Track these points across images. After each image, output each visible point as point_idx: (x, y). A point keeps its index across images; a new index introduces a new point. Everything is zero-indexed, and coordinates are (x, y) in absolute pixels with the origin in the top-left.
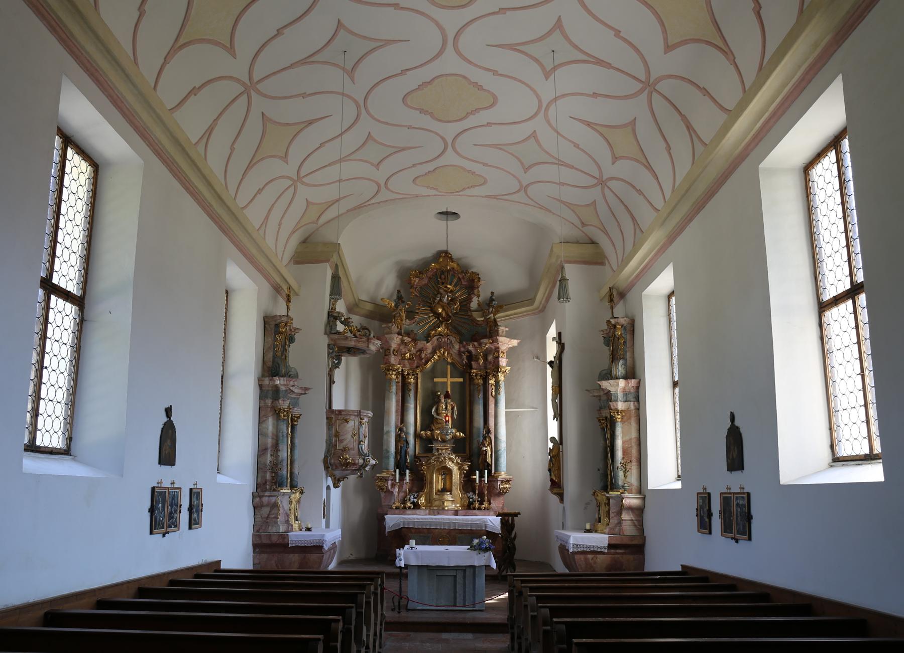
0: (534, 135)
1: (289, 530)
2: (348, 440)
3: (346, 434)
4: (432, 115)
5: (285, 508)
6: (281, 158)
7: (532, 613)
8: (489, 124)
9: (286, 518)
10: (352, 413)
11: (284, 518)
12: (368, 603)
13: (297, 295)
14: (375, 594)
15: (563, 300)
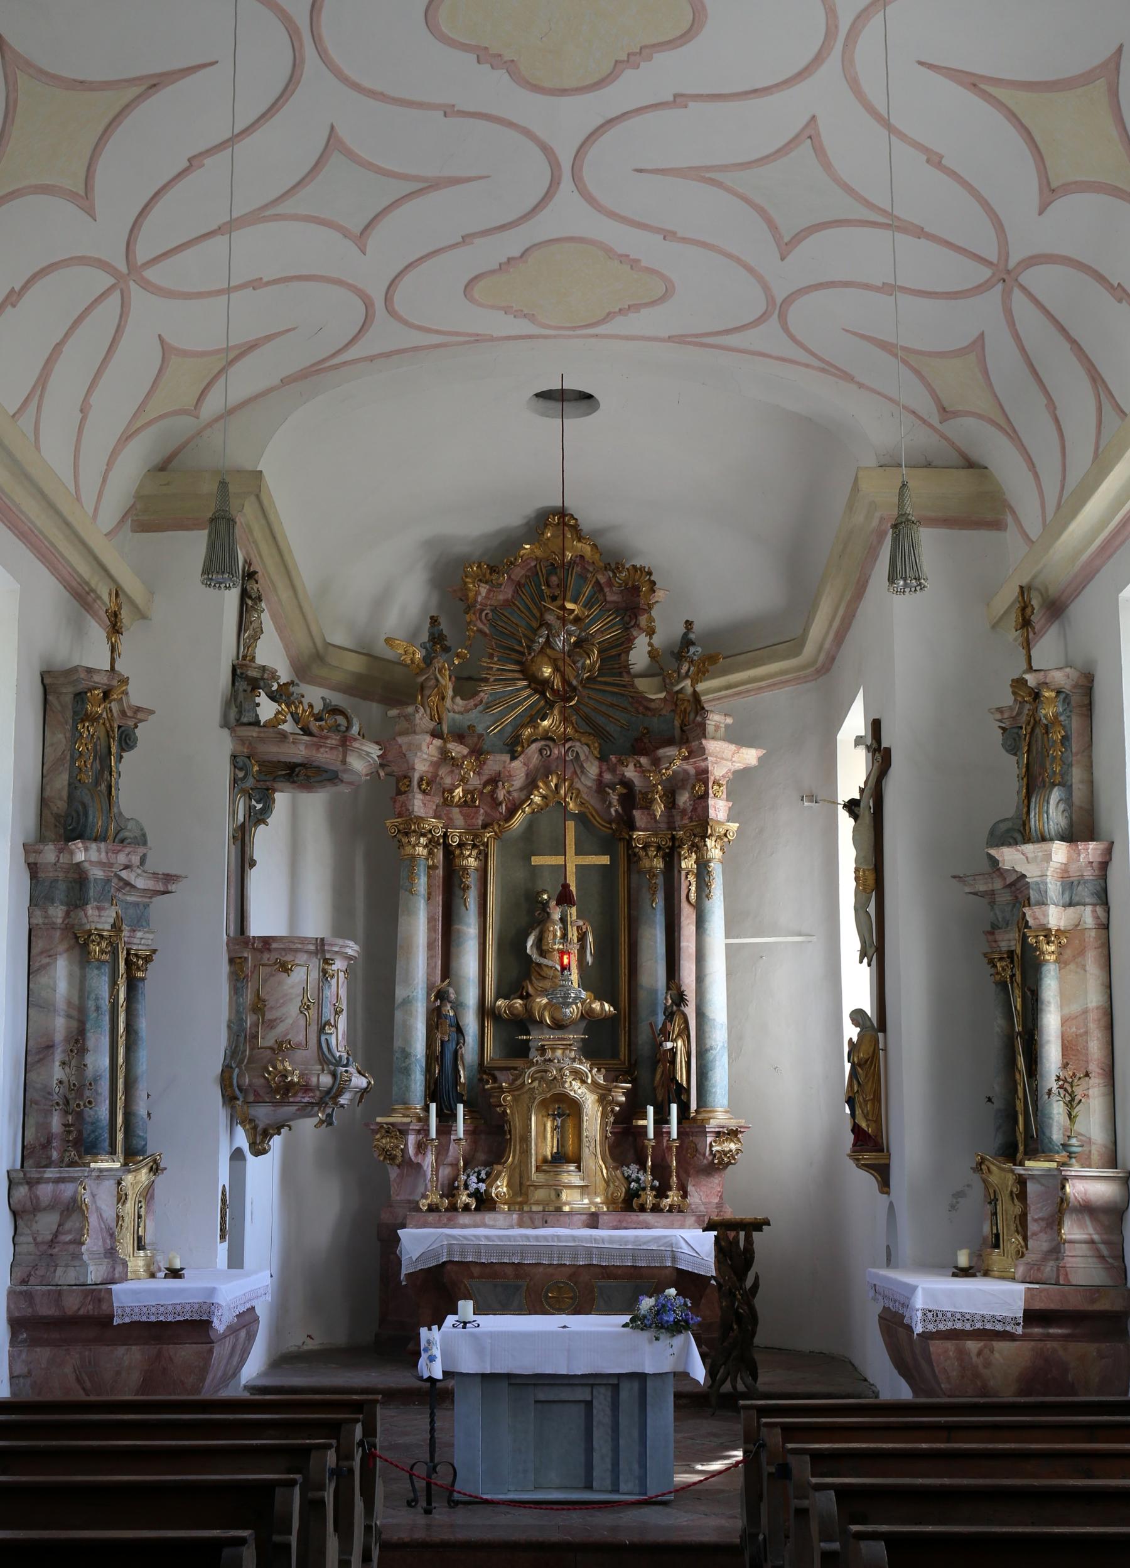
0: (810, 133)
1: (117, 1275)
2: (290, 1021)
3: (283, 1004)
4: (511, 68)
5: (105, 1215)
6: (71, 196)
7: (822, 1544)
8: (680, 100)
9: (108, 1242)
10: (299, 946)
11: (100, 1243)
12: (312, 1507)
13: (144, 617)
14: (342, 1475)
15: (906, 585)
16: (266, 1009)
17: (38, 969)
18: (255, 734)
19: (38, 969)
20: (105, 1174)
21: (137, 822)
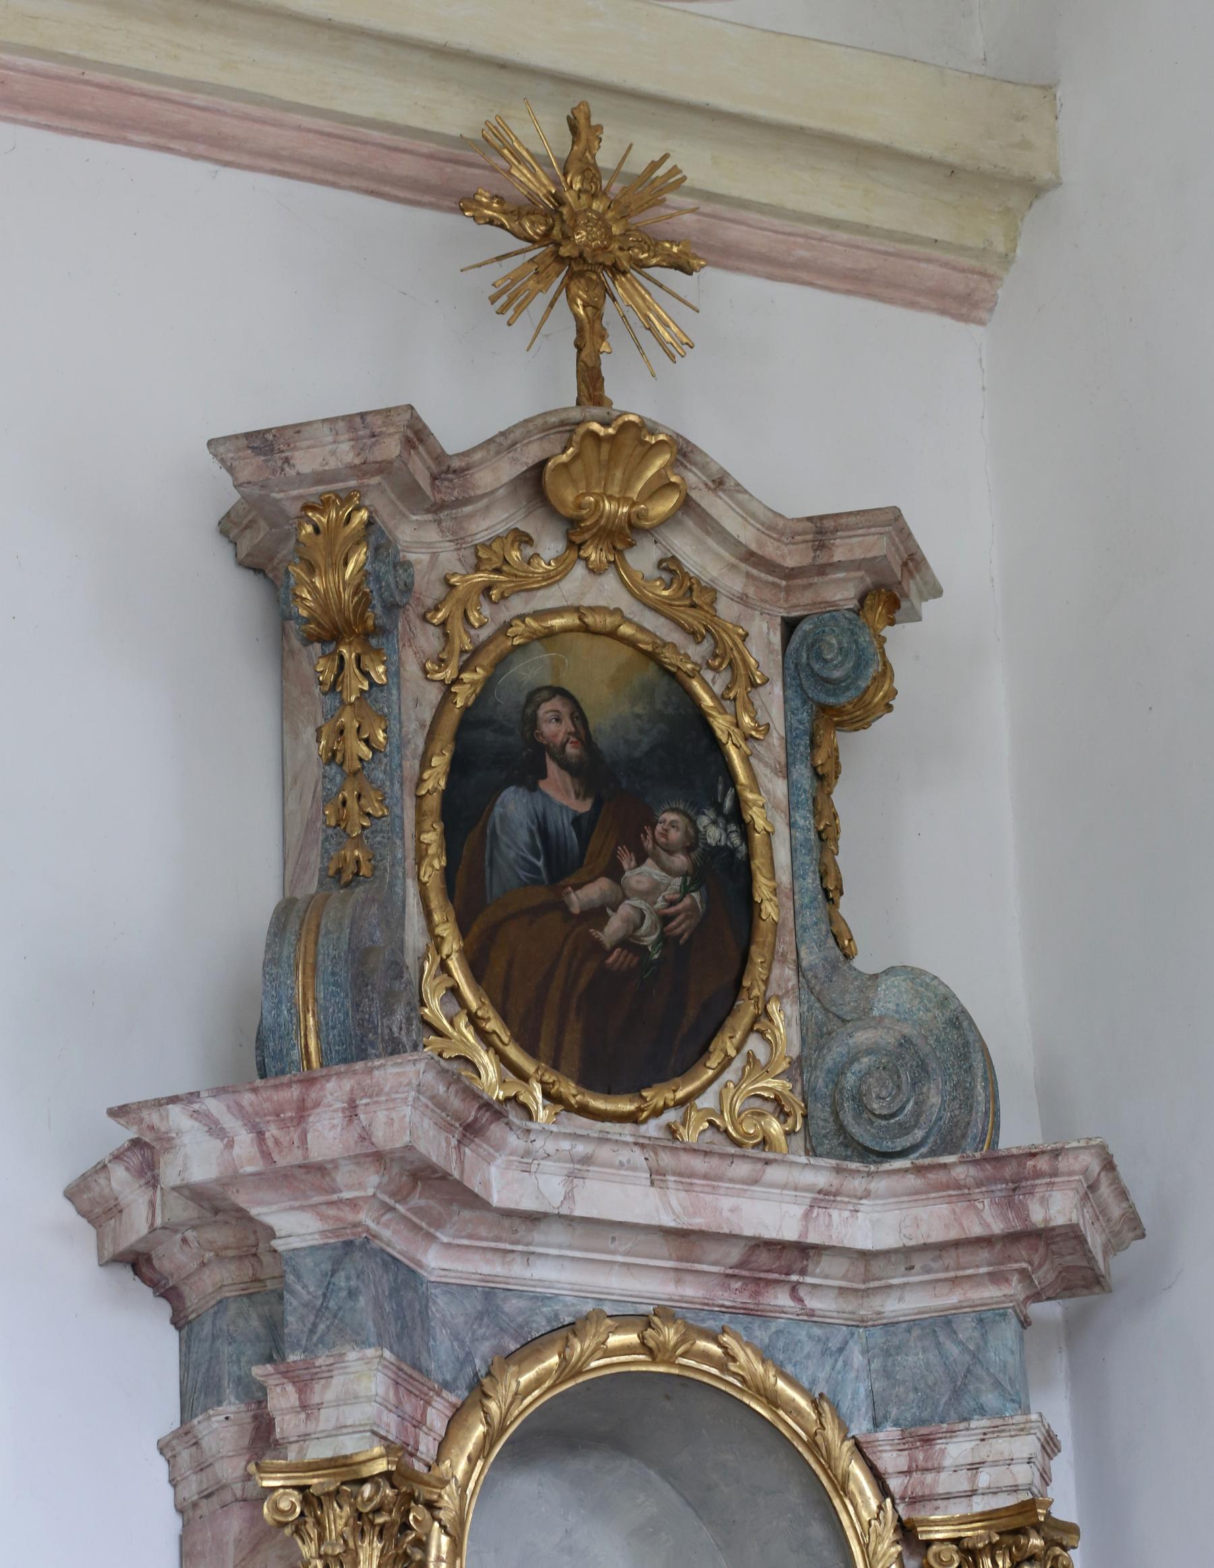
13: (1034, 189)
21: (914, 975)
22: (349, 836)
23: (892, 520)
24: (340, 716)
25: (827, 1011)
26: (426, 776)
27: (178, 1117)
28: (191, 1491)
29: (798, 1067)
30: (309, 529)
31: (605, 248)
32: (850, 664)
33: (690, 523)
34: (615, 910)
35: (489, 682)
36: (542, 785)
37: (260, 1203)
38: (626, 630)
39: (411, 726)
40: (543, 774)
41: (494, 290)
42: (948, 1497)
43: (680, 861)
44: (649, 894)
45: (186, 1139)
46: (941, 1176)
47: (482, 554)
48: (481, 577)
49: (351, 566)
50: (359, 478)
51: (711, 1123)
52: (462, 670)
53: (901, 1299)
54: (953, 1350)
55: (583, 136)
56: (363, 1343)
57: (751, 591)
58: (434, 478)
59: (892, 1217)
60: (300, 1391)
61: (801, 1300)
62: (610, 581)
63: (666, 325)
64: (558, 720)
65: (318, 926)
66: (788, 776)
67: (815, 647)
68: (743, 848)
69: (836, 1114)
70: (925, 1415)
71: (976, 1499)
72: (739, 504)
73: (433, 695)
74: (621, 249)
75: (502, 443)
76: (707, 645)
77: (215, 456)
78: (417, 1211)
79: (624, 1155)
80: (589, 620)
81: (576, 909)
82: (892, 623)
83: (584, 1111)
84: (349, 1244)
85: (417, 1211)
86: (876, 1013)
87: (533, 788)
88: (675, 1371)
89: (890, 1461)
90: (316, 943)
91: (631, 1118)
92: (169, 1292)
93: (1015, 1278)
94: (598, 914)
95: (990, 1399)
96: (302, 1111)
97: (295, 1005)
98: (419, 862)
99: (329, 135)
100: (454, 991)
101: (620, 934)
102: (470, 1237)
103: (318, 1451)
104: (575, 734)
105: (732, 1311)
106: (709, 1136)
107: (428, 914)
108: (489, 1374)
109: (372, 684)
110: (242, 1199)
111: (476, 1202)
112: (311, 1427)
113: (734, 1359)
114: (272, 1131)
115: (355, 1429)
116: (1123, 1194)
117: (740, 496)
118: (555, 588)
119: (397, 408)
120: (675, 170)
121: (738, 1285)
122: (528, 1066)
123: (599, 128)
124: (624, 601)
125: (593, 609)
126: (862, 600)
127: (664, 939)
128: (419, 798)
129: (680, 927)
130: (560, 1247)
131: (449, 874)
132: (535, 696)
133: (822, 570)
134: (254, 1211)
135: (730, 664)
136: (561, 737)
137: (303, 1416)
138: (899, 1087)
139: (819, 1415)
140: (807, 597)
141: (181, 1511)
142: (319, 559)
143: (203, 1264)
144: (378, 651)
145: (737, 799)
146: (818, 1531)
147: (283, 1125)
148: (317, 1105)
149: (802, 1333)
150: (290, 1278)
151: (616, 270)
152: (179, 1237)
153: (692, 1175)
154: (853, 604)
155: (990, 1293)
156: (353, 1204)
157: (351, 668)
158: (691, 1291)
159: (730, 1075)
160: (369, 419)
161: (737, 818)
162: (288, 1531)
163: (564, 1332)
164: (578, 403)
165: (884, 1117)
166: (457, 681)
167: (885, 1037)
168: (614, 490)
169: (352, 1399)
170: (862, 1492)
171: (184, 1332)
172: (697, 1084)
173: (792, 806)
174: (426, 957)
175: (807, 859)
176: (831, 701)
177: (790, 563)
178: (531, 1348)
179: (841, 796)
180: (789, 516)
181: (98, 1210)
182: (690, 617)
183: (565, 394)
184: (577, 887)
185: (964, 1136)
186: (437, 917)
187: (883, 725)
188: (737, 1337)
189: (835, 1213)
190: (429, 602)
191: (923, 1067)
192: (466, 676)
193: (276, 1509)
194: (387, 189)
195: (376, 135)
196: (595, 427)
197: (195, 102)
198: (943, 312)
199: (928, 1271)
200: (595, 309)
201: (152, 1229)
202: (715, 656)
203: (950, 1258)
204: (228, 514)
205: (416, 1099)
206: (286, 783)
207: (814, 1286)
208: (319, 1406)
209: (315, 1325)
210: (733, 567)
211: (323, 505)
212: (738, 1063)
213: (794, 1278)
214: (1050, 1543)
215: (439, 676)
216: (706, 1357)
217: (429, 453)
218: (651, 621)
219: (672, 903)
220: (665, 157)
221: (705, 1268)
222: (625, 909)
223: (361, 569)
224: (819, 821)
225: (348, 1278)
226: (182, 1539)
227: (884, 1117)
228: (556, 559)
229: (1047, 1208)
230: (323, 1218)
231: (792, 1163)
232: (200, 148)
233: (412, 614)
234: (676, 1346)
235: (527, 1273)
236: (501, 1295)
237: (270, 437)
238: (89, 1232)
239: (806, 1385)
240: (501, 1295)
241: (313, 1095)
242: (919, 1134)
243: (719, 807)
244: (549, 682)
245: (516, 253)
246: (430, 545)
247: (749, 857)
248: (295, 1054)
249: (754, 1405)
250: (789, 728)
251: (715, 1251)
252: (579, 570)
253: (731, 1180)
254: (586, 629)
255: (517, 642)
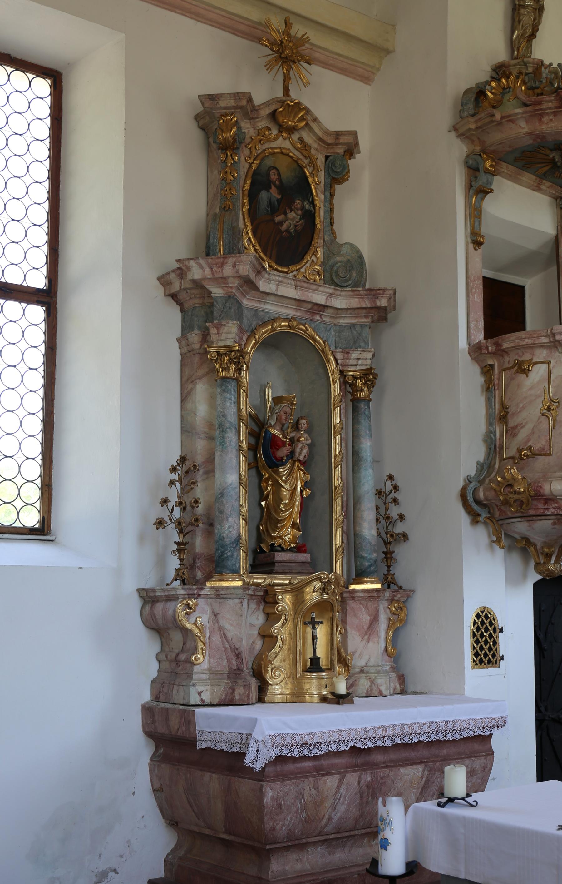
2: (530, 426)
3: (523, 407)
5: (229, 635)
10: (530, 341)
13: (388, 52)
16: (509, 416)
17: (186, 396)
18: (473, 126)
19: (186, 396)
20: (222, 592)
21: (351, 245)
22: (227, 199)
23: (354, 134)
24: (226, 169)
25: (330, 251)
26: (245, 186)
27: (192, 263)
28: (185, 350)
29: (322, 264)
30: (222, 121)
31: (291, 56)
32: (341, 168)
33: (307, 129)
34: (285, 223)
35: (260, 164)
36: (270, 190)
37: (209, 285)
38: (291, 154)
39: (242, 173)
40: (271, 188)
41: (265, 64)
42: (351, 365)
43: (300, 212)
44: (293, 219)
45: (194, 269)
46: (357, 293)
47: (260, 131)
48: (259, 137)
49: (232, 132)
50: (234, 109)
51: (304, 275)
52: (254, 160)
53: (344, 320)
54: (355, 333)
55: (288, 25)
56: (232, 320)
57: (319, 148)
58: (251, 111)
59: (345, 301)
60: (217, 330)
61: (322, 318)
62: (287, 142)
63: (304, 78)
64: (275, 175)
65: (224, 220)
66: (324, 194)
67: (333, 163)
68: (313, 211)
69: (331, 276)
70: (347, 347)
71: (357, 366)
72: (319, 125)
73: (247, 166)
74: (296, 57)
75: (267, 104)
76: (308, 160)
77: (199, 99)
78: (244, 290)
79: (290, 281)
80: (283, 151)
81: (276, 222)
82: (350, 159)
83: (276, 270)
84: (229, 297)
85: (244, 290)
86: (341, 253)
87: (268, 191)
88: (295, 332)
89: (339, 356)
90: (223, 224)
91: (287, 273)
92: (180, 304)
93: (370, 317)
94: (281, 223)
95: (362, 344)
96: (222, 265)
97: (218, 239)
98: (243, 206)
99: (225, 17)
100: (249, 239)
101: (286, 229)
102: (253, 297)
103: (221, 344)
104: (278, 179)
105: (307, 319)
106: (303, 278)
107: (244, 220)
108: (255, 329)
109: (234, 162)
110: (205, 284)
111: (256, 289)
112: (219, 338)
113: (308, 330)
114: (215, 269)
115: (230, 339)
116: (395, 301)
117: (320, 124)
118: (275, 142)
119: (247, 92)
120: (308, 37)
121: (309, 313)
122: (265, 258)
123: (292, 24)
124: (290, 147)
125: (284, 148)
126: (345, 152)
127: (295, 231)
128: (243, 191)
129: (299, 228)
130: (272, 301)
131: (249, 210)
132: (270, 168)
133: (336, 144)
134: (207, 287)
135: (313, 166)
136: (275, 179)
137: (218, 335)
138: (346, 271)
139: (325, 345)
140: (331, 151)
141: (181, 354)
142: (224, 128)
143: (191, 298)
144: (236, 154)
145: (313, 198)
146: (321, 371)
147: (218, 267)
148: (226, 263)
149: (321, 326)
150: (215, 303)
151: (294, 62)
152: (186, 291)
153: (303, 287)
154: (342, 154)
155: (364, 320)
156: (231, 287)
157: (229, 157)
158: (299, 314)
159: (308, 264)
160: (239, 94)
161: (313, 203)
162: (214, 361)
163: (272, 321)
164: (284, 96)
165: (343, 278)
166: (253, 163)
167: (343, 259)
168: (291, 119)
169: (229, 332)
170: (332, 363)
171: (183, 313)
172: (301, 266)
173: (325, 202)
174: (244, 230)
175: (328, 215)
176: (336, 177)
177: (329, 142)
178: (264, 324)
179: (335, 201)
180: (330, 130)
181: (165, 283)
182: (305, 153)
183: (280, 93)
184: (277, 216)
185: (360, 284)
186: (246, 220)
187: (345, 184)
188: (308, 325)
189: (333, 299)
190: (247, 143)
191: (352, 267)
192: (255, 162)
193: (211, 355)
194: (236, 33)
195: (236, 18)
196: (289, 102)
197: (193, 3)
198: (361, 81)
199: (351, 314)
200: (288, 71)
201: (181, 288)
202: (310, 163)
203: (356, 311)
204: (198, 114)
205: (250, 264)
206: (209, 183)
207: (326, 315)
208: (222, 333)
209: (221, 315)
210: (315, 141)
211: (226, 115)
212: (310, 262)
213: (321, 313)
214: (374, 378)
215: (248, 161)
216: (301, 329)
217: (251, 104)
218: (296, 153)
219: (297, 222)
220: (306, 33)
221: (303, 309)
222: (287, 223)
223: (234, 133)
224: (331, 206)
225: (229, 304)
226: (181, 361)
227: (343, 278)
228: (276, 135)
229: (381, 302)
230: (224, 290)
231: (325, 287)
232: (193, 16)
233: (243, 145)
234: (296, 326)
235: (264, 307)
236: (258, 311)
237: (214, 96)
238: (162, 288)
239: (322, 337)
240: (258, 311)
241: (226, 261)
242: (350, 282)
243: (309, 200)
244: (273, 165)
245: (271, 55)
246: (248, 128)
247: (315, 213)
248: (217, 250)
249: (311, 341)
250: (325, 183)
251: (306, 305)
252: (281, 138)
253: (312, 289)
254: (282, 153)
255: (267, 155)
